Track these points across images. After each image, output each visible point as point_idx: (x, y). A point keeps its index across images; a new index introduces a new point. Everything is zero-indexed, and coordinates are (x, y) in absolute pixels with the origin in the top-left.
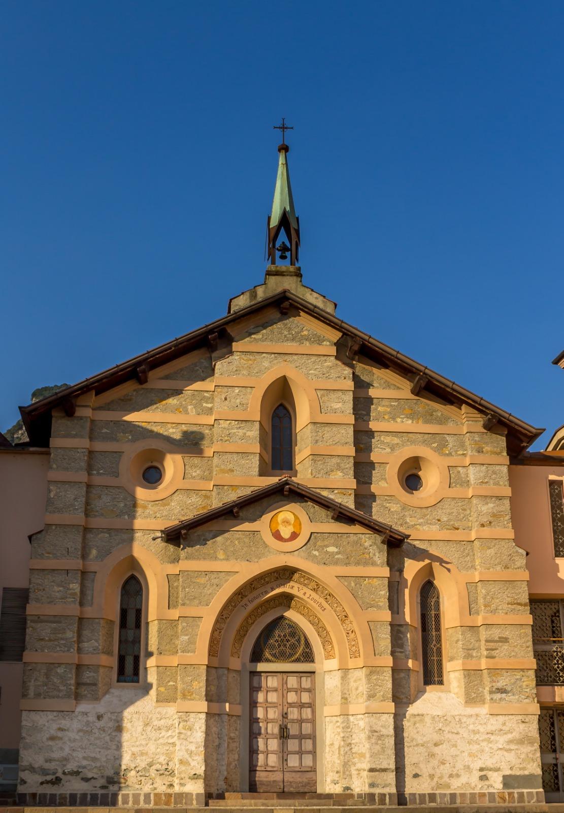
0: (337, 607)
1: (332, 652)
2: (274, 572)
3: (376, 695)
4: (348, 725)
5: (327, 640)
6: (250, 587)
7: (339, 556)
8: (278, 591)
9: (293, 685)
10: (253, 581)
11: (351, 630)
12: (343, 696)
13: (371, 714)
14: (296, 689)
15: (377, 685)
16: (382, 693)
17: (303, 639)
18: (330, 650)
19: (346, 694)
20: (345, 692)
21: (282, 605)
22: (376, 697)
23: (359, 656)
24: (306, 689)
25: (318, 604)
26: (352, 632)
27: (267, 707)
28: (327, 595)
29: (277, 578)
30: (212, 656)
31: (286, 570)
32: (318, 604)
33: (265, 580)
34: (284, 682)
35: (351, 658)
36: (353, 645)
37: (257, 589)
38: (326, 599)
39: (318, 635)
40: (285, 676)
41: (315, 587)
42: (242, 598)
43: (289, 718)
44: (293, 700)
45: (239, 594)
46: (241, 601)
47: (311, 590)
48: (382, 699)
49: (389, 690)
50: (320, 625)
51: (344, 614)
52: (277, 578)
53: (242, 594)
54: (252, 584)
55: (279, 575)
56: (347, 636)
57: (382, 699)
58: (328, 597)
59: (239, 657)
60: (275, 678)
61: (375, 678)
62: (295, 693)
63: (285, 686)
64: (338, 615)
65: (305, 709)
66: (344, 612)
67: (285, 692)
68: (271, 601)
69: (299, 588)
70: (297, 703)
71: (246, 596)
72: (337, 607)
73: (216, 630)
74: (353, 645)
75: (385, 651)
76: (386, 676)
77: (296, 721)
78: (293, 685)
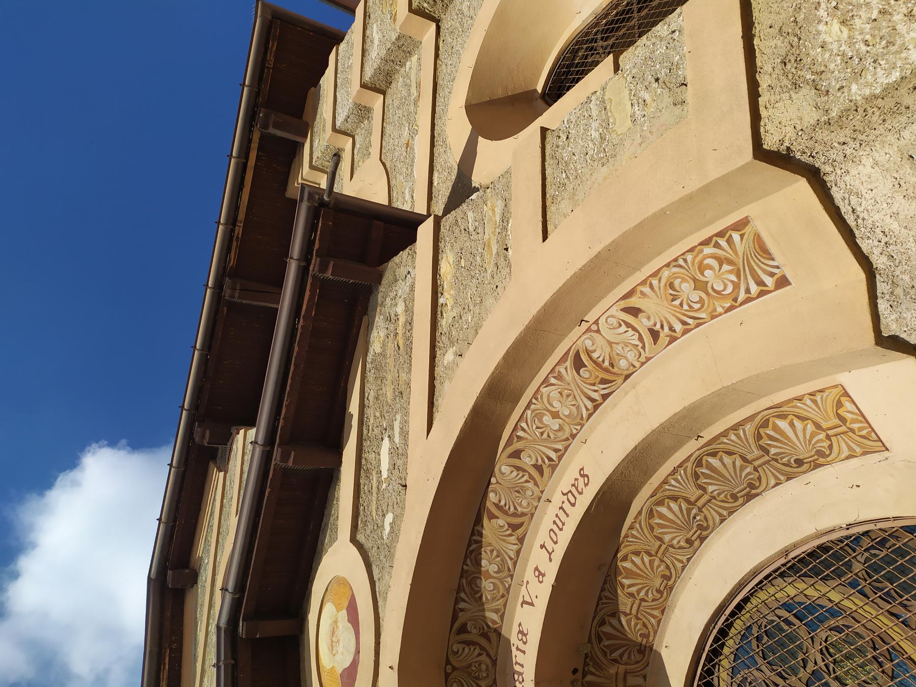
0: (555, 415)
1: (807, 408)
5: (757, 452)
11: (630, 319)
17: (790, 589)
18: (810, 427)
23: (740, 226)
25: (567, 506)
26: (635, 312)
28: (518, 468)
31: (448, 662)
32: (567, 506)
35: (783, 282)
36: (700, 285)
38: (539, 468)
39: (749, 497)
41: (501, 522)
47: (521, 540)
50: (693, 493)
51: (569, 374)
56: (673, 339)
58: (527, 460)
64: (590, 405)
66: (559, 377)
72: (555, 415)
74: (700, 285)
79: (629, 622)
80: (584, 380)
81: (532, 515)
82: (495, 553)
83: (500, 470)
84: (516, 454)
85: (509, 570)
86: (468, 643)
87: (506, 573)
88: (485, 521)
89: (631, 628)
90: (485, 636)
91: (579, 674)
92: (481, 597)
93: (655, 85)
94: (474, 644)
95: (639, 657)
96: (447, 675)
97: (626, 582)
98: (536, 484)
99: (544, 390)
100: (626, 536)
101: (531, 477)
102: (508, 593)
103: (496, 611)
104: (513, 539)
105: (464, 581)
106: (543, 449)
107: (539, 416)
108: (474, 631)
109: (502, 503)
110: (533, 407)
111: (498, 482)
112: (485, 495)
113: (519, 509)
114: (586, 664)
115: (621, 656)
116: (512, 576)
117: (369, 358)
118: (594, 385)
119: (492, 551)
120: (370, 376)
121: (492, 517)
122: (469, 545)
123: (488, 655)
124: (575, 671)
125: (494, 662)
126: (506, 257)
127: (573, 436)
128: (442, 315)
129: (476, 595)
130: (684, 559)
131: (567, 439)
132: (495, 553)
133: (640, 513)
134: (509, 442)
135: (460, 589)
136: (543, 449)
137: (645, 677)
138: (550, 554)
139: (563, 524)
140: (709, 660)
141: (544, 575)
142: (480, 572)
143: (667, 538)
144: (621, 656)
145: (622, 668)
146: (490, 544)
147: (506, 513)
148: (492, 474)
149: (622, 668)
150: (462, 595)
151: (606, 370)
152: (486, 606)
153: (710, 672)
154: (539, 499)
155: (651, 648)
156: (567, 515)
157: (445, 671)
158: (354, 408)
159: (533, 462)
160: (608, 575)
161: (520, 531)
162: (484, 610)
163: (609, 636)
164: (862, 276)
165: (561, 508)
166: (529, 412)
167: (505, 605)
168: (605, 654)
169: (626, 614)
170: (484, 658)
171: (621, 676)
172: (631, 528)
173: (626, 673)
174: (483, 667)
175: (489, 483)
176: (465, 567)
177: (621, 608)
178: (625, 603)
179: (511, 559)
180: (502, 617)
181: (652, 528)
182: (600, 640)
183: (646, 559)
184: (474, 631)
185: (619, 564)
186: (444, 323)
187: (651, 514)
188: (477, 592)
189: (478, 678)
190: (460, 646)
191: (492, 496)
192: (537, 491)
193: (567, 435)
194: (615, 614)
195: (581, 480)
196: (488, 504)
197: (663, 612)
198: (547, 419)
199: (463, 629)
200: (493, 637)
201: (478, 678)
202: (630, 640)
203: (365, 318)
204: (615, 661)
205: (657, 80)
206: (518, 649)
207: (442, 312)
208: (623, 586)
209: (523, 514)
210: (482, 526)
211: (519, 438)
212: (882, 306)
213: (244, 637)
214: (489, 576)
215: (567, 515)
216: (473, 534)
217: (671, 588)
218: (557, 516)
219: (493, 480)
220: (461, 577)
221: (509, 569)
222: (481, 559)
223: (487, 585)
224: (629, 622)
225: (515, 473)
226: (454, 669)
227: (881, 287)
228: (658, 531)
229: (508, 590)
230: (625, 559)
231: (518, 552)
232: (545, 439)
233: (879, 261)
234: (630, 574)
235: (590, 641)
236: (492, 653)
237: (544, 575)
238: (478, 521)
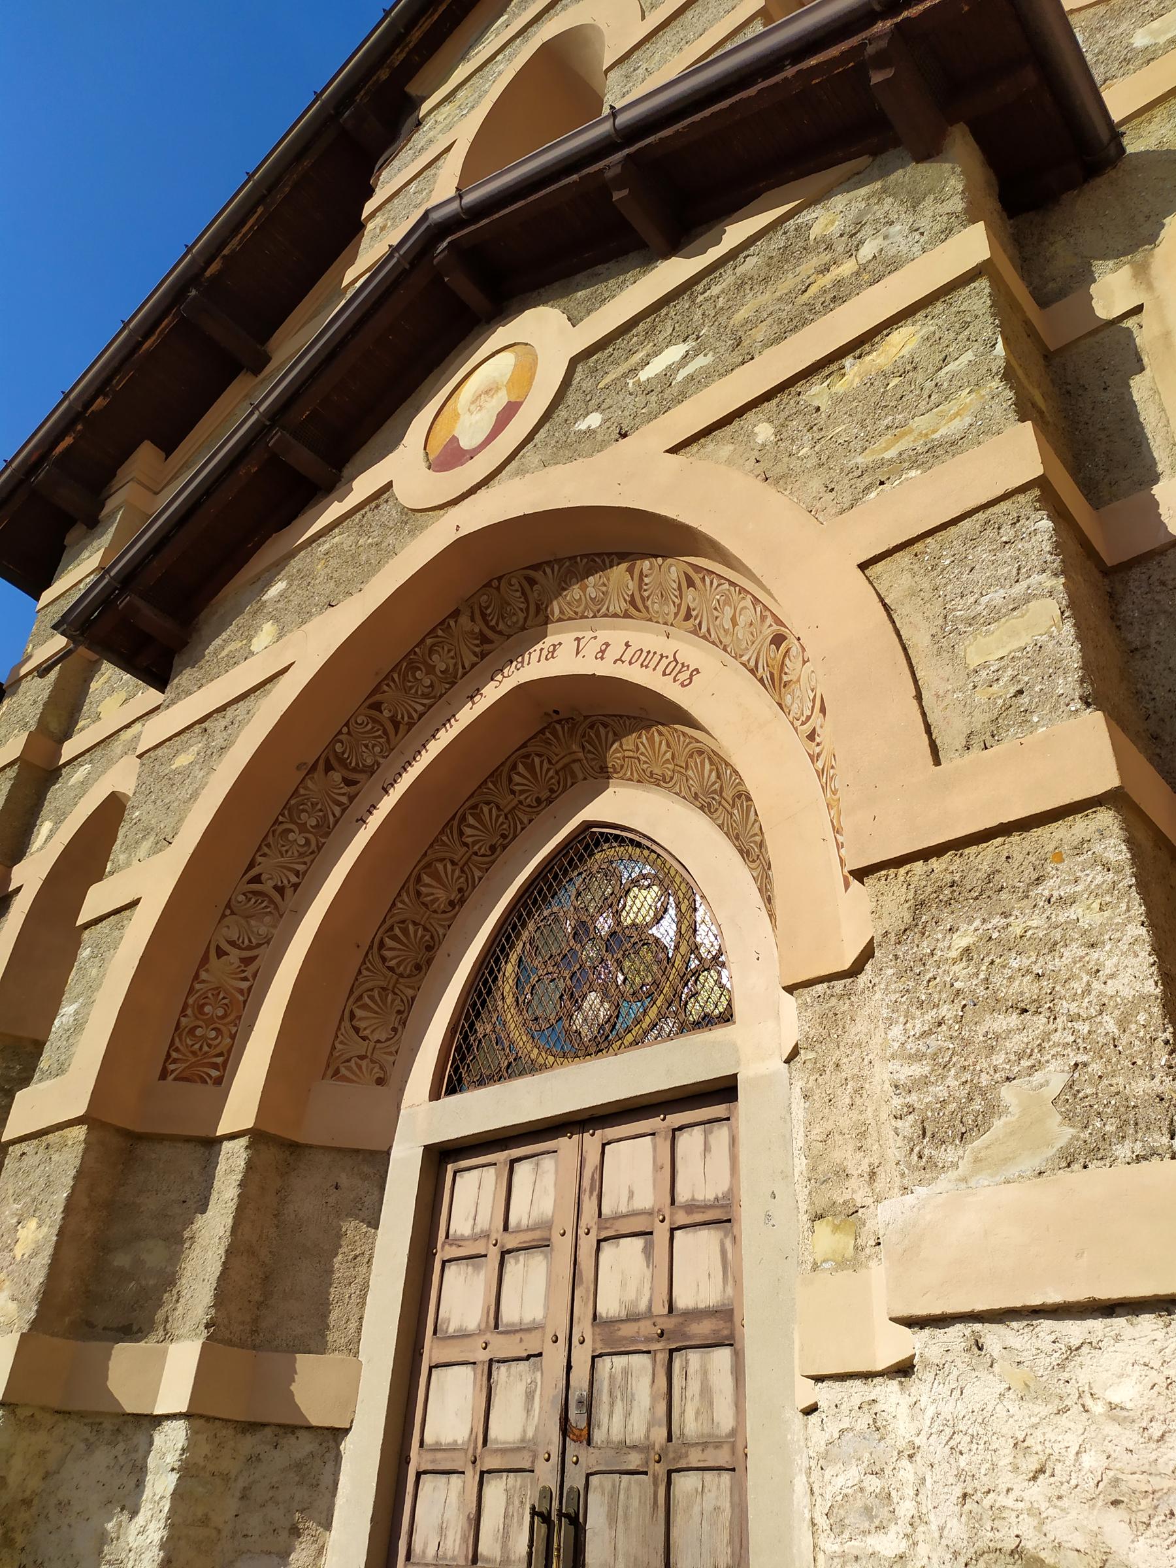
2: (456, 614)
3: (993, 1109)
4: (873, 1484)
6: (375, 721)
7: (701, 361)
8: (492, 693)
9: (631, 1195)
10: (376, 690)
12: (821, 1203)
13: (957, 1331)
14: (650, 1213)
15: (996, 1005)
16: (1054, 1077)
19: (842, 1174)
20: (837, 1156)
21: (573, 776)
22: (998, 1124)
24: (706, 1207)
27: (491, 1361)
29: (485, 640)
30: (175, 1079)
31: (500, 579)
33: (431, 669)
34: (586, 1183)
37: (411, 725)
39: (741, 851)
40: (591, 1141)
42: (349, 782)
43: (598, 1436)
44: (631, 1295)
45: (329, 768)
46: (352, 799)
47: (627, 615)
48: (1065, 1134)
49: (1123, 1023)
52: (485, 640)
53: (343, 762)
54: (377, 706)
55: (483, 615)
57: (1065, 1134)
59: (380, 1082)
60: (548, 1163)
61: (961, 941)
62: (639, 1242)
63: (589, 1206)
65: (694, 1357)
67: (587, 1244)
68: (514, 767)
69: (578, 639)
70: (649, 1314)
71: (371, 771)
73: (221, 953)
75: (1025, 699)
76: (1067, 902)
77: (634, 1461)
78: (631, 1195)
79: (616, 751)
80: (768, 651)
81: (650, 620)
82: (604, 589)
83: (671, 566)
84: (691, 583)
85: (599, 611)
86: (524, 593)
87: (595, 609)
88: (624, 566)
89: (614, 754)
90: (538, 609)
91: (556, 717)
92: (565, 589)
93: (1013, 690)
94: (527, 601)
95: (597, 768)
96: (488, 585)
97: (644, 739)
98: (676, 614)
99: (748, 602)
100: (676, 730)
101: (679, 606)
102: (581, 618)
103: (562, 612)
104: (624, 605)
105: (567, 564)
106: (705, 613)
107: (728, 602)
108: (536, 594)
109: (646, 580)
110: (732, 588)
111: (660, 566)
112: (645, 556)
113: (649, 603)
114: (567, 720)
115: (589, 752)
116: (595, 616)
117: (805, 217)
118: (768, 666)
119: (604, 585)
120: (778, 240)
121: (630, 570)
122: (599, 555)
123: (526, 619)
124: (556, 712)
125: (523, 628)
126: (867, 489)
127: (725, 650)
128: (827, 377)
129: (563, 586)
130: (683, 794)
131: (721, 642)
132: (604, 589)
133: (698, 741)
134: (697, 569)
135: (559, 561)
136: (705, 613)
137: (585, 779)
138: (620, 659)
139: (647, 667)
140: (616, 837)
141: (602, 658)
142: (582, 579)
143: (690, 773)
144: (589, 752)
145: (581, 755)
146: (608, 580)
147: (640, 588)
148: (664, 557)
149: (581, 755)
150: (556, 567)
151: (781, 678)
152: (560, 598)
153: (607, 841)
154: (665, 624)
155: (609, 778)
156: (654, 669)
157: (492, 580)
158: (735, 233)
159: (692, 606)
160: (642, 719)
161: (632, 611)
162: (556, 598)
163: (598, 735)
164: (846, 966)
165: (662, 656)
166: (726, 586)
167: (570, 619)
168: (584, 736)
169: (621, 746)
170: (522, 615)
171: (574, 757)
172: (684, 734)
173: (579, 760)
174: (514, 619)
175: (656, 556)
176: (579, 558)
177: (624, 740)
178: (629, 741)
179: (608, 609)
180: (560, 620)
181: (691, 756)
182: (591, 727)
183: (668, 755)
184: (536, 594)
185: (654, 729)
186: (817, 392)
187: (701, 753)
188: (565, 583)
189: (503, 618)
190: (517, 587)
191: (646, 564)
192: (671, 618)
193: (726, 641)
194: (618, 737)
195: (687, 675)
196: (639, 562)
197: (639, 781)
198: (729, 612)
199: (532, 582)
200: (541, 618)
201: (503, 618)
202: (605, 757)
203: (865, 160)
204: (583, 748)
205: (1021, 692)
206: (542, 650)
207: (830, 375)
208: (640, 737)
209: (647, 608)
210: (618, 564)
211: (703, 580)
212: (820, 988)
213: (435, 261)
214: (584, 589)
215: (654, 669)
216: (609, 554)
217: (658, 785)
218: (655, 653)
219: (660, 559)
220: (570, 558)
221: (598, 611)
222: (592, 575)
223: (575, 592)
224: (616, 751)
225: (675, 586)
226: (498, 589)
227: (839, 985)
228: (691, 762)
229: (583, 617)
230: (660, 734)
231: (615, 615)
232: (712, 614)
233: (862, 979)
234: (651, 740)
235: (586, 717)
236: (529, 623)
237: (602, 658)
238: (622, 557)
